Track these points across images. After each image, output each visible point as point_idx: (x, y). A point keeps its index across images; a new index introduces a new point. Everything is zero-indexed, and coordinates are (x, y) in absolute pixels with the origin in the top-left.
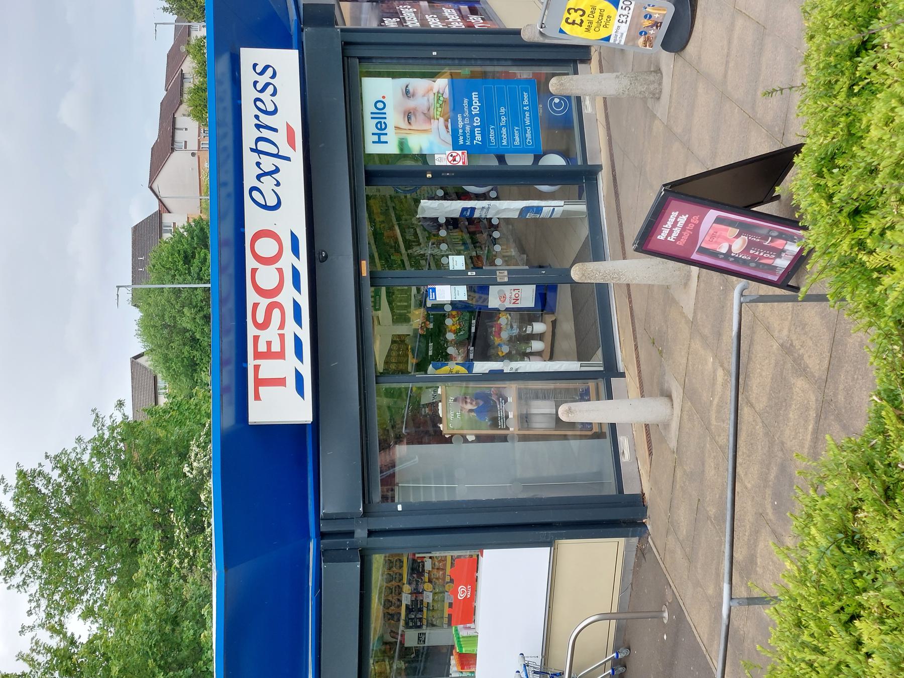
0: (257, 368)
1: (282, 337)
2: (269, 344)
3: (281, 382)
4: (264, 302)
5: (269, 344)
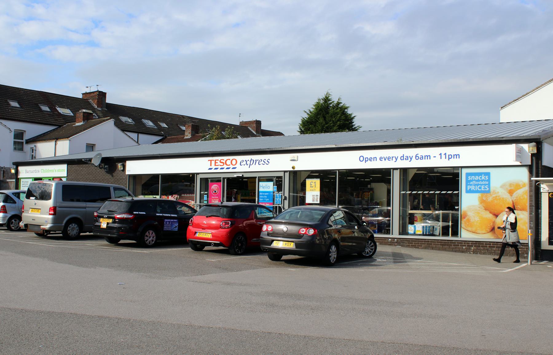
0: (213, 160)
1: (218, 165)
2: (217, 163)
3: (211, 165)
4: (224, 162)
5: (217, 163)
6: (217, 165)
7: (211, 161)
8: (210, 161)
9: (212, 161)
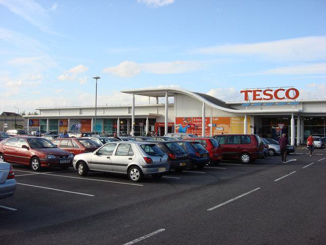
0: (251, 91)
1: (261, 99)
2: (259, 95)
4: (272, 93)
5: (259, 95)
6: (258, 99)
7: (246, 92)
8: (244, 93)
9: (248, 93)
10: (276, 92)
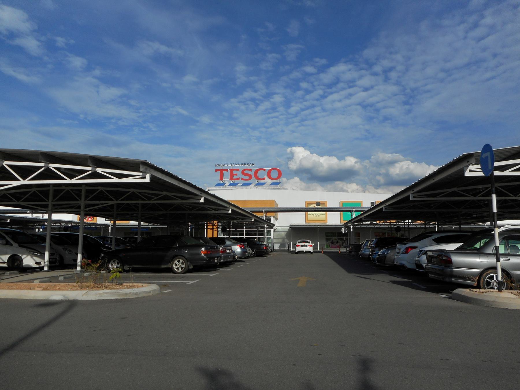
0: (227, 170)
1: (238, 179)
2: (236, 175)
3: (221, 179)
4: (252, 173)
5: (236, 175)
7: (222, 171)
9: (224, 172)
10: (256, 172)
